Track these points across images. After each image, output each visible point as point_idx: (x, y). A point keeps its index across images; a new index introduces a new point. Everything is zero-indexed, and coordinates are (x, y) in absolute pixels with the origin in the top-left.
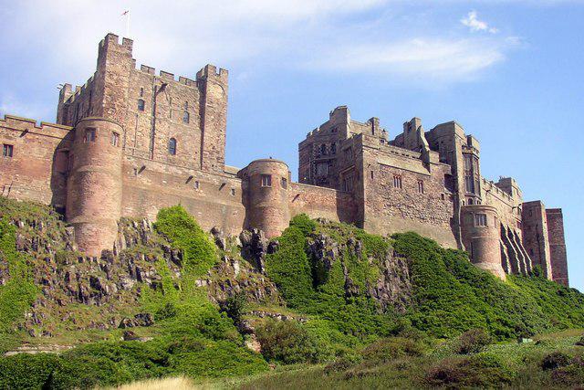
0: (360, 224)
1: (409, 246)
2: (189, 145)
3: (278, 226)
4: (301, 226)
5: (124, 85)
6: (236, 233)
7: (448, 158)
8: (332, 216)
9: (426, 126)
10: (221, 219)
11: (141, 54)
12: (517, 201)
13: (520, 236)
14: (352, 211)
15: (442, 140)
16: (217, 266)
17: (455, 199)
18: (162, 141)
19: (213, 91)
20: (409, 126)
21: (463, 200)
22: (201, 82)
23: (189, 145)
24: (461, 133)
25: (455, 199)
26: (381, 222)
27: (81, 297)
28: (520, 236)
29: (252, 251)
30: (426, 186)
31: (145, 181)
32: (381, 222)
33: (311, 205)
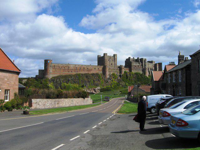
0: (131, 71)
1: (136, 74)
2: (113, 63)
3: (123, 73)
4: (125, 72)
5: (106, 58)
6: (119, 74)
7: (142, 62)
8: (128, 71)
9: (140, 58)
10: (117, 73)
11: (108, 55)
12: (154, 63)
13: (154, 69)
14: (130, 70)
15: (142, 60)
16: (117, 78)
17: (143, 68)
18: (111, 64)
19: (115, 57)
20: (138, 58)
21: (144, 67)
22: (114, 55)
23: (113, 63)
24: (144, 59)
25: (143, 68)
26: (134, 71)
27: (107, 82)
28: (154, 69)
29: (120, 76)
30: (139, 66)
31: (110, 70)
32: (134, 71)
33: (126, 70)
